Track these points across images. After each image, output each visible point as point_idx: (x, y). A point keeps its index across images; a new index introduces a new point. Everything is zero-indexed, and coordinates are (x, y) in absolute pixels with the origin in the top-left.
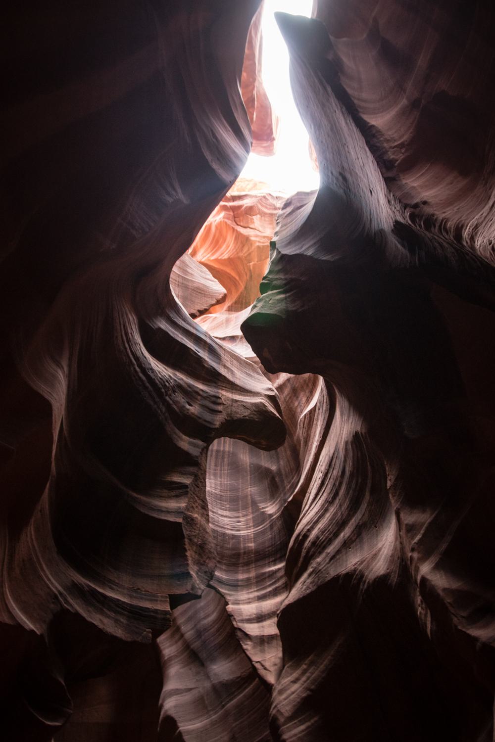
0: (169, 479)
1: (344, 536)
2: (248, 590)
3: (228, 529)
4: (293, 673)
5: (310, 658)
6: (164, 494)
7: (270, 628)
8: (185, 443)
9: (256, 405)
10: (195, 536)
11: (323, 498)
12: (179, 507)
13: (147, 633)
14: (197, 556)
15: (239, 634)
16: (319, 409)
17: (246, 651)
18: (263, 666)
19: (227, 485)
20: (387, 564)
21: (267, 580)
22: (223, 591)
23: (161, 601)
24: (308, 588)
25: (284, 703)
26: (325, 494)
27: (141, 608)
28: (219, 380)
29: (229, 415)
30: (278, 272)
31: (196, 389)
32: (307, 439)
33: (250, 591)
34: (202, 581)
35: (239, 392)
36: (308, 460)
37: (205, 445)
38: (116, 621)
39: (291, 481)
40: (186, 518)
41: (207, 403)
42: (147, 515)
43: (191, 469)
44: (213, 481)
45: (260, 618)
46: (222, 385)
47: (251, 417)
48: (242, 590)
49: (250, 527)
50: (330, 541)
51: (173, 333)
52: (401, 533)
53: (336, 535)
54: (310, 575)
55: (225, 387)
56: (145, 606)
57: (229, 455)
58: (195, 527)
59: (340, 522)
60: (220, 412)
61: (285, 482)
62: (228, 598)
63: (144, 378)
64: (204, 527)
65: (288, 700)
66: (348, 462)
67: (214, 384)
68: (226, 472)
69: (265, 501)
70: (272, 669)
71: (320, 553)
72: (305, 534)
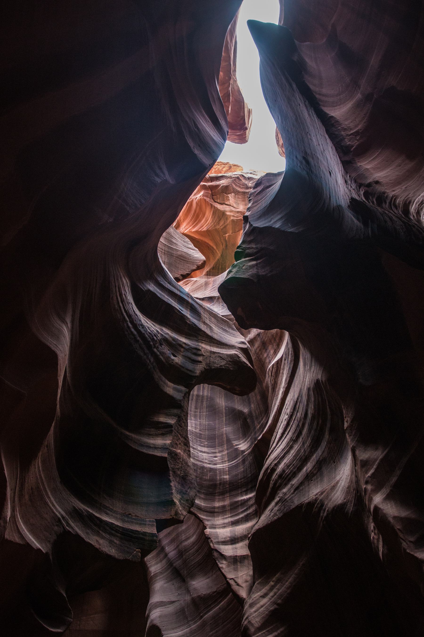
0: (156, 419)
1: (306, 470)
2: (223, 516)
3: (206, 463)
4: (262, 589)
5: (277, 576)
6: (152, 433)
7: (241, 549)
8: (170, 389)
9: (231, 356)
10: (178, 469)
11: (288, 437)
12: (165, 444)
13: (137, 552)
14: (180, 486)
15: (215, 554)
16: (285, 360)
17: (221, 569)
18: (236, 582)
19: (206, 425)
20: (344, 494)
21: (240, 507)
22: (202, 516)
23: (148, 525)
24: (275, 514)
25: (254, 615)
26: (290, 434)
27: (132, 531)
28: (199, 334)
29: (208, 365)
30: (250, 242)
31: (179, 342)
32: (275, 386)
33: (225, 517)
34: (184, 508)
35: (217, 345)
36: (275, 404)
37: (187, 390)
38: (111, 542)
39: (260, 422)
40: (171, 454)
41: (189, 354)
42: (138, 451)
43: (175, 411)
44: (193, 421)
45: (233, 540)
46: (202, 339)
47: (227, 367)
48: (218, 516)
49: (225, 461)
50: (294, 475)
51: (160, 294)
52: (356, 468)
53: (300, 469)
54: (277, 504)
55: (205, 341)
56: (135, 529)
57: (207, 399)
58: (179, 461)
59: (304, 458)
60: (200, 362)
61: (256, 422)
62: (206, 523)
63: (135, 333)
64: (186, 461)
65: (258, 612)
66: (310, 406)
67: (195, 338)
68: (205, 413)
69: (238, 439)
70: (244, 585)
71: (286, 485)
72: (272, 468)
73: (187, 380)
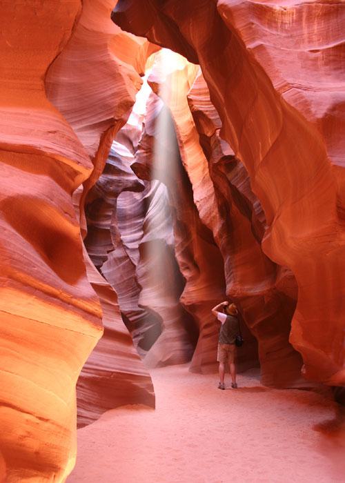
9: (134, 181)
30: (145, 141)
41: (116, 184)
73: (116, 195)
